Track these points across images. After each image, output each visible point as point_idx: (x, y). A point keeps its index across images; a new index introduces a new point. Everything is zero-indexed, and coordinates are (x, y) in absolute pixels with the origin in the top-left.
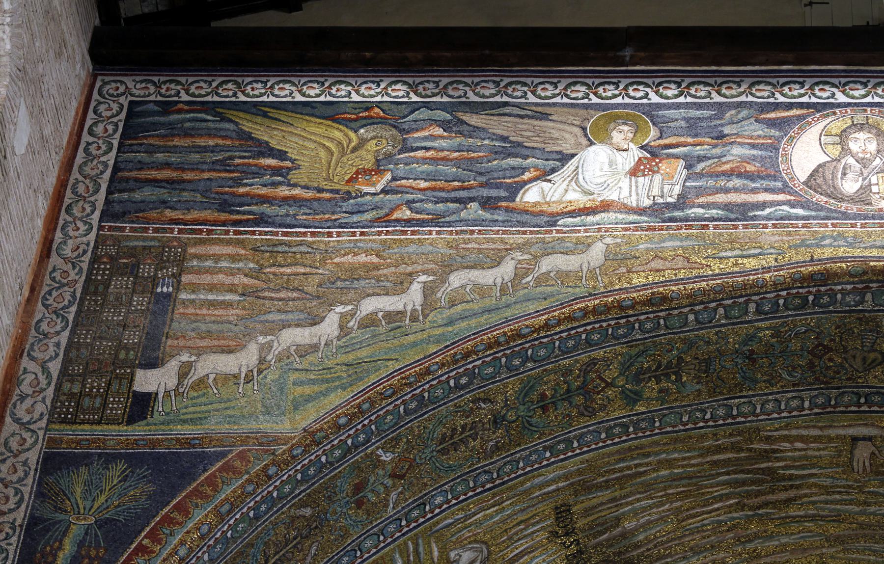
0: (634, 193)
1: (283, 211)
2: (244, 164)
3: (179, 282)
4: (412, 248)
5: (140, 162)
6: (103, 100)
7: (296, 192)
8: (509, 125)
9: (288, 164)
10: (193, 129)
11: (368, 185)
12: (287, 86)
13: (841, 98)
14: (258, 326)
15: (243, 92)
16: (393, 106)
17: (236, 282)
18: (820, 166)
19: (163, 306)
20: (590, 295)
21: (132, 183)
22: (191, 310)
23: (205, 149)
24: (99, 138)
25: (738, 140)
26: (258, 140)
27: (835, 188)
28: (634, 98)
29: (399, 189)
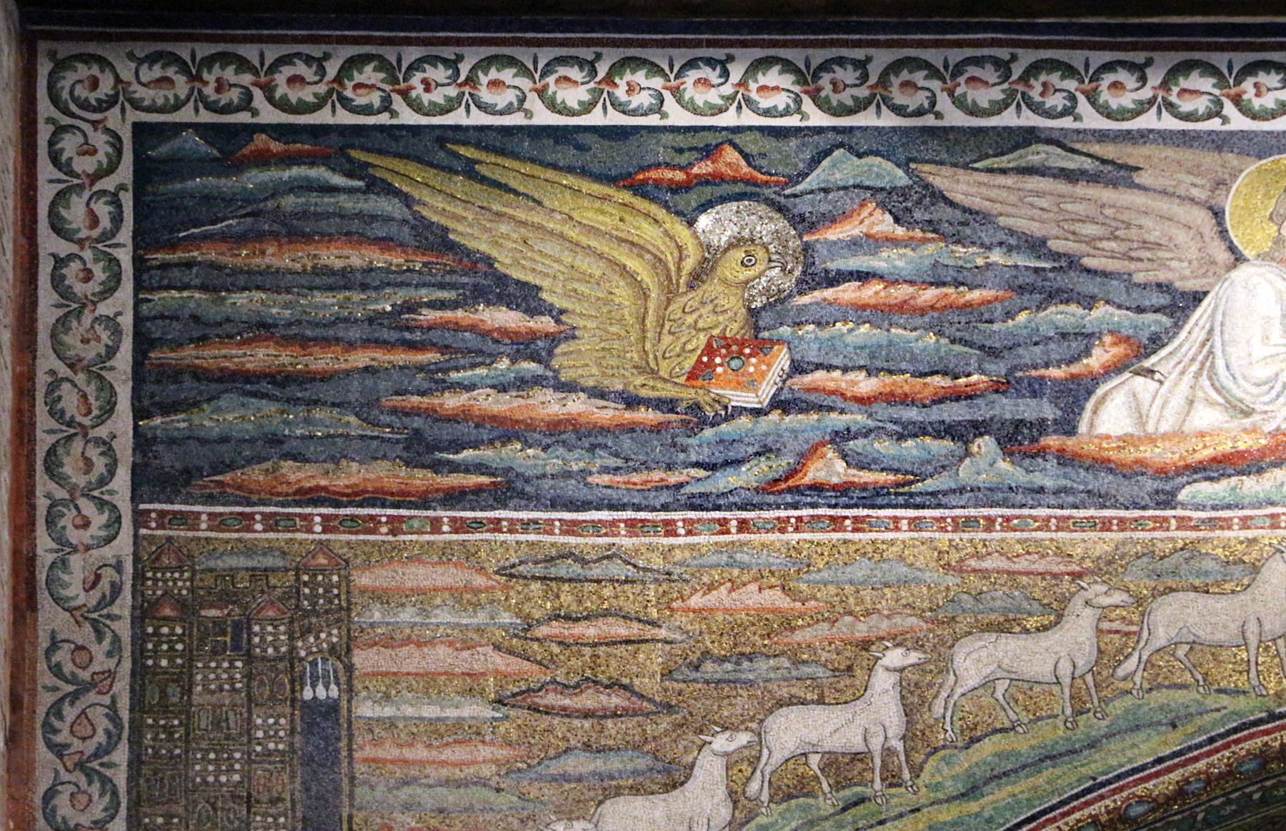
1: (553, 463)
2: (443, 326)
3: (350, 669)
4: (860, 570)
5: (195, 318)
6: (66, 120)
7: (577, 405)
8: (1043, 203)
9: (545, 323)
10: (304, 214)
11: (739, 385)
12: (507, 75)
14: (549, 792)
15: (404, 94)
16: (769, 144)
17: (478, 667)
19: (326, 739)
20: (1273, 717)
21: (188, 382)
22: (389, 751)
23: (343, 280)
24: (81, 242)
26: (468, 253)
29: (812, 397)
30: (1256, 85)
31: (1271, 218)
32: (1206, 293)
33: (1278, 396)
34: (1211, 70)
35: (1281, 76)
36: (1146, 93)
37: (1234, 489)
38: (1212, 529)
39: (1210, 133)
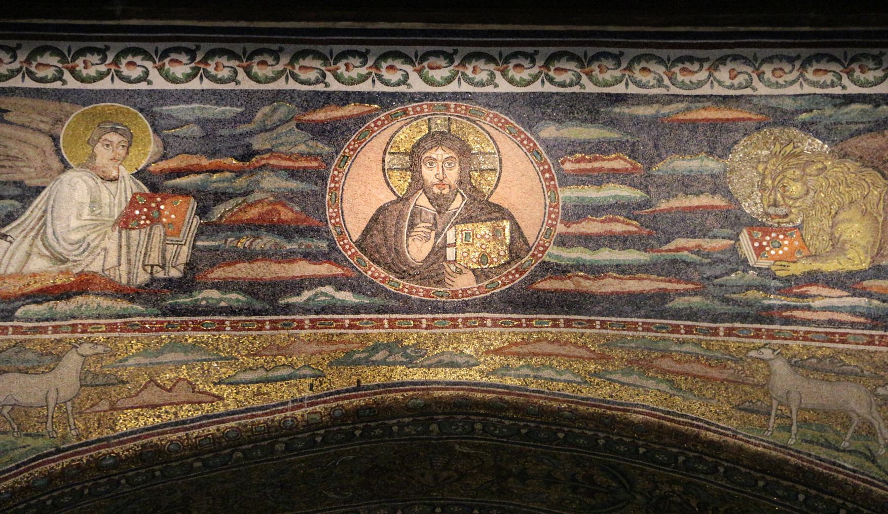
0: (124, 260)
13: (417, 85)
18: (382, 210)
20: (58, 451)
25: (273, 162)
27: (397, 252)
28: (128, 80)
30: (85, 62)
31: (88, 143)
32: (44, 188)
33: (84, 251)
34: (56, 52)
35: (100, 57)
36: (16, 65)
37: (51, 308)
38: (34, 333)
39: (54, 90)
